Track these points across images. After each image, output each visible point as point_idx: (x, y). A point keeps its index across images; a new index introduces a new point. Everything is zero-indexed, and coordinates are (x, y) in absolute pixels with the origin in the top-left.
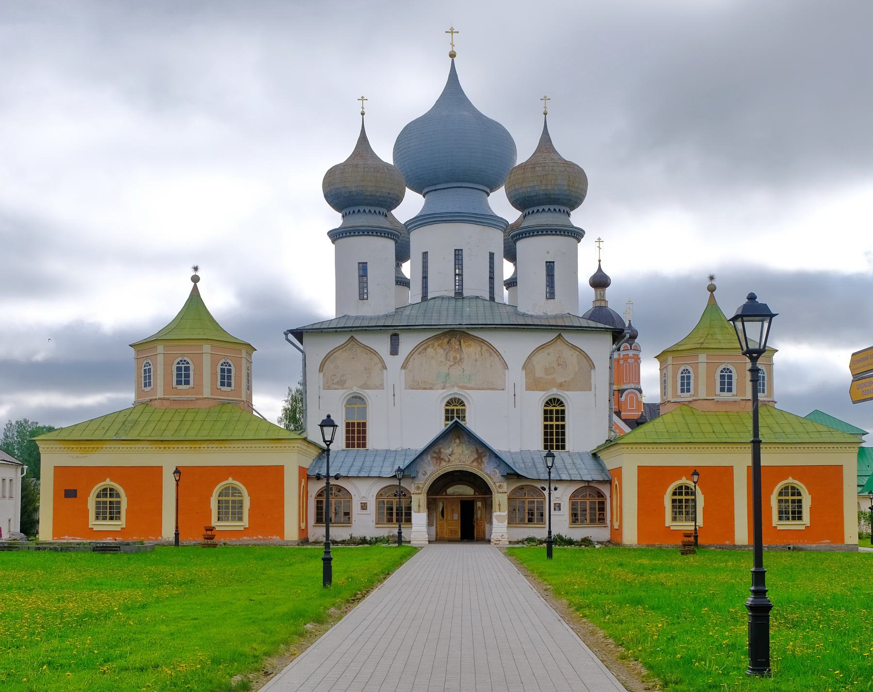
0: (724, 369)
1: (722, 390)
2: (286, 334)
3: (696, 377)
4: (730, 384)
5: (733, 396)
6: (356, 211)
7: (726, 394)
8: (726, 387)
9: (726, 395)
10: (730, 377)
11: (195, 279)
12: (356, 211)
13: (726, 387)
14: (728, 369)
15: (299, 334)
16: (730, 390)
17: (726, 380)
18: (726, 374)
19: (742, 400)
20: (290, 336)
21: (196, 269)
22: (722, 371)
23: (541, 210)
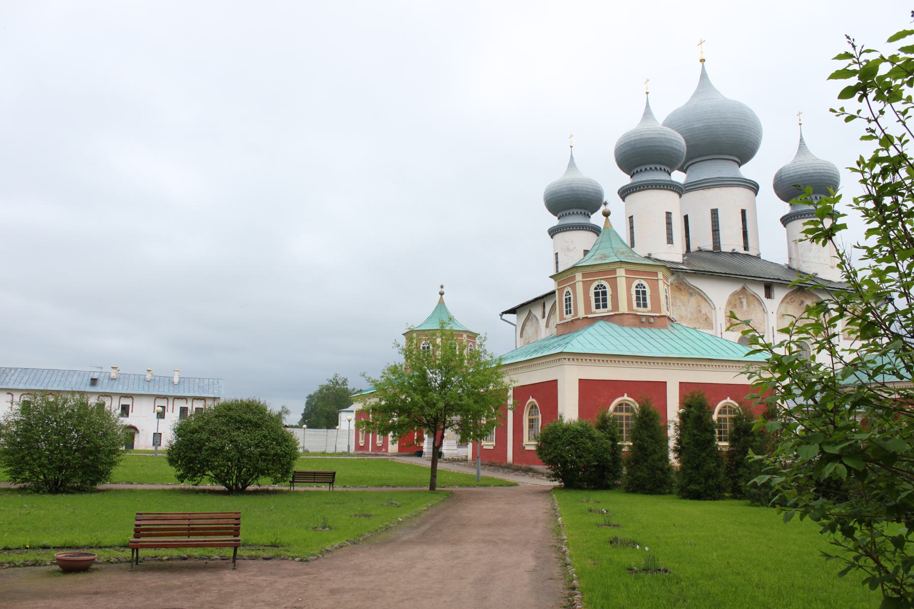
0: (598, 286)
1: (598, 307)
2: (501, 315)
3: (575, 297)
4: (605, 300)
5: (608, 312)
6: (568, 214)
7: (602, 310)
8: (601, 303)
9: (602, 312)
10: (604, 293)
11: (442, 294)
12: (568, 214)
13: (601, 303)
14: (602, 285)
15: (513, 311)
16: (605, 306)
17: (601, 297)
18: (600, 291)
19: (615, 315)
20: (505, 316)
21: (442, 287)
22: (596, 289)
23: (648, 169)
